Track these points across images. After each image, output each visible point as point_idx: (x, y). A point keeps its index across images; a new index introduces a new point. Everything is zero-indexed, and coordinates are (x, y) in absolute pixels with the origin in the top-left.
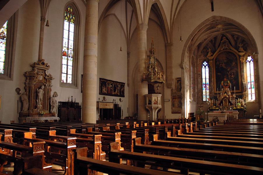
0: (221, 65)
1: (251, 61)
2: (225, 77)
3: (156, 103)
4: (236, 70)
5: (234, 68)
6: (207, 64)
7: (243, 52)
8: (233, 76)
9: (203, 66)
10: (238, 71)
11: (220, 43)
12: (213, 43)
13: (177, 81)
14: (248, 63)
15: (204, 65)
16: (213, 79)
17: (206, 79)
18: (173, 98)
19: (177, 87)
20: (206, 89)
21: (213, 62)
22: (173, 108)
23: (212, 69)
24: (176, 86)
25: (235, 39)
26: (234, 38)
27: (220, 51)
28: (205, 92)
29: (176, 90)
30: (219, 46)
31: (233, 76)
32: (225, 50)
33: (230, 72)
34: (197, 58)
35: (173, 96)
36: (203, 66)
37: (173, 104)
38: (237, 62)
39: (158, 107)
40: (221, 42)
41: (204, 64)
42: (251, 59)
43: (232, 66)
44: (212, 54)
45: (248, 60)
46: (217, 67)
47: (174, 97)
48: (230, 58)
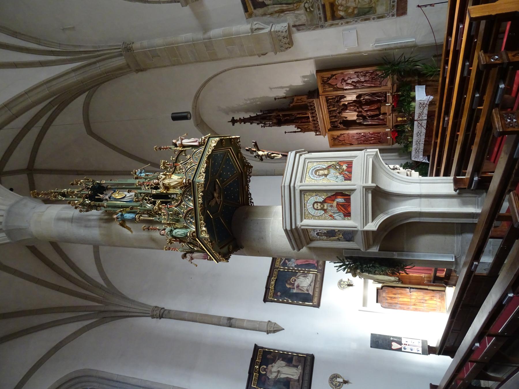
3: (340, 200)
13: (260, 11)
18: (334, 17)
19: (285, 7)
22: (380, 9)
24: (282, 11)
29: (297, 9)
35: (326, 20)
37: (359, 15)
39: (367, 189)
47: (329, 14)
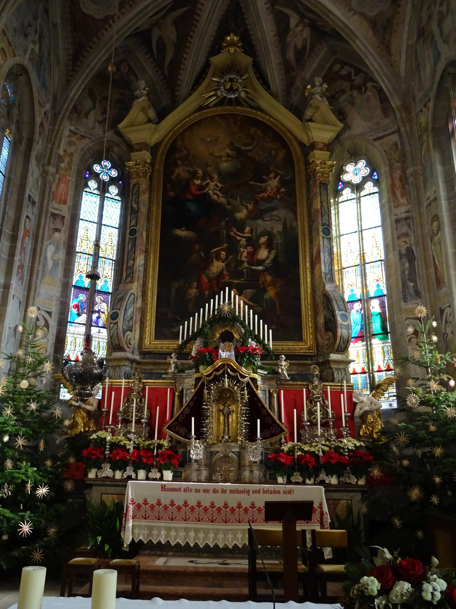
0: (198, 182)
1: (369, 187)
2: (218, 258)
4: (285, 224)
5: (274, 209)
6: (114, 173)
7: (326, 123)
8: (263, 254)
9: (93, 184)
10: (296, 228)
11: (207, 65)
12: (167, 61)
14: (347, 193)
15: (96, 176)
16: (140, 260)
17: (96, 256)
20: (89, 324)
21: (152, 164)
23: (145, 197)
25: (291, 55)
26: (283, 51)
27: (200, 108)
28: (81, 340)
30: (197, 83)
31: (263, 254)
32: (227, 109)
33: (248, 229)
34: (56, 116)
36: (93, 184)
38: (293, 179)
40: (216, 60)
41: (97, 168)
42: (366, 171)
43: (265, 195)
44: (152, 114)
45: (346, 178)
46: (172, 194)
48: (249, 154)
